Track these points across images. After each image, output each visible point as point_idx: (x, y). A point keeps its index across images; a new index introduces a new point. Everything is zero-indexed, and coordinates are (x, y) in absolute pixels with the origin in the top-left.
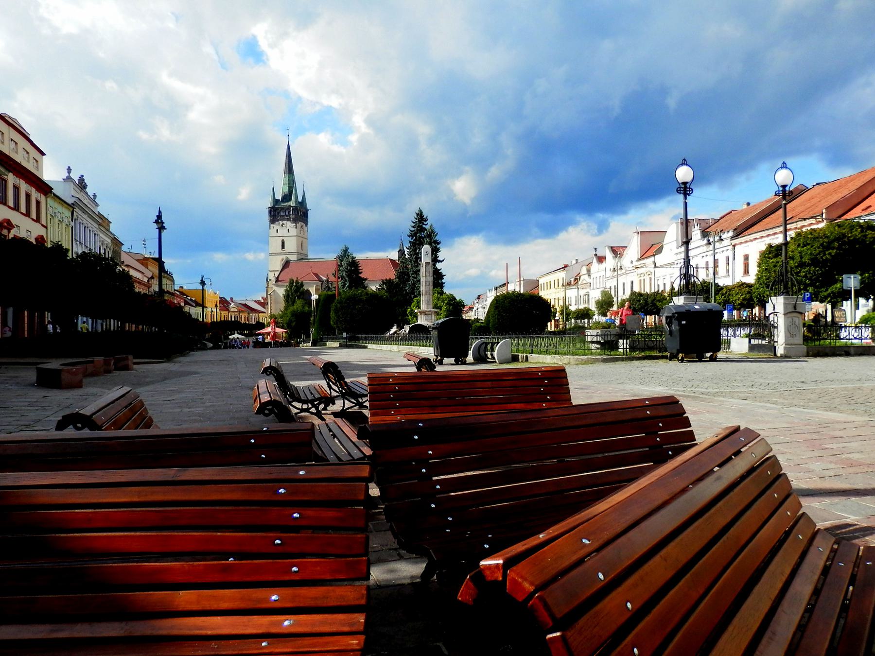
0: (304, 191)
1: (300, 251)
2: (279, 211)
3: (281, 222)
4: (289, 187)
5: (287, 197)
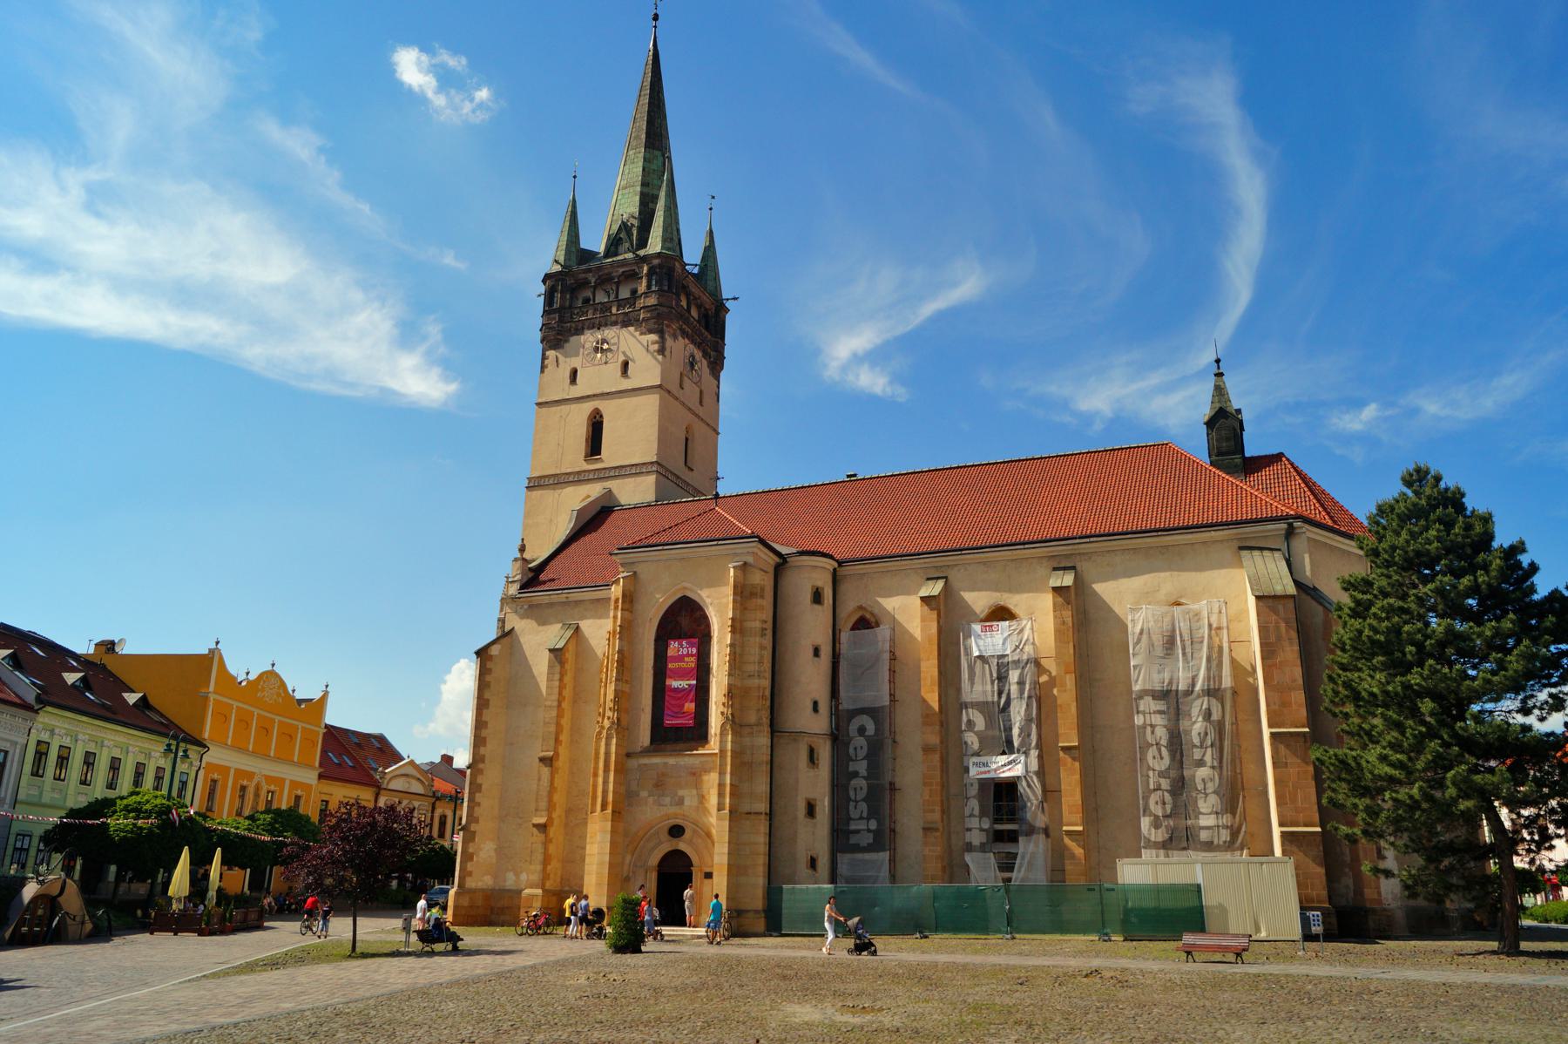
0: (711, 232)
1: (677, 465)
2: (588, 294)
3: (589, 338)
4: (643, 195)
5: (630, 234)
